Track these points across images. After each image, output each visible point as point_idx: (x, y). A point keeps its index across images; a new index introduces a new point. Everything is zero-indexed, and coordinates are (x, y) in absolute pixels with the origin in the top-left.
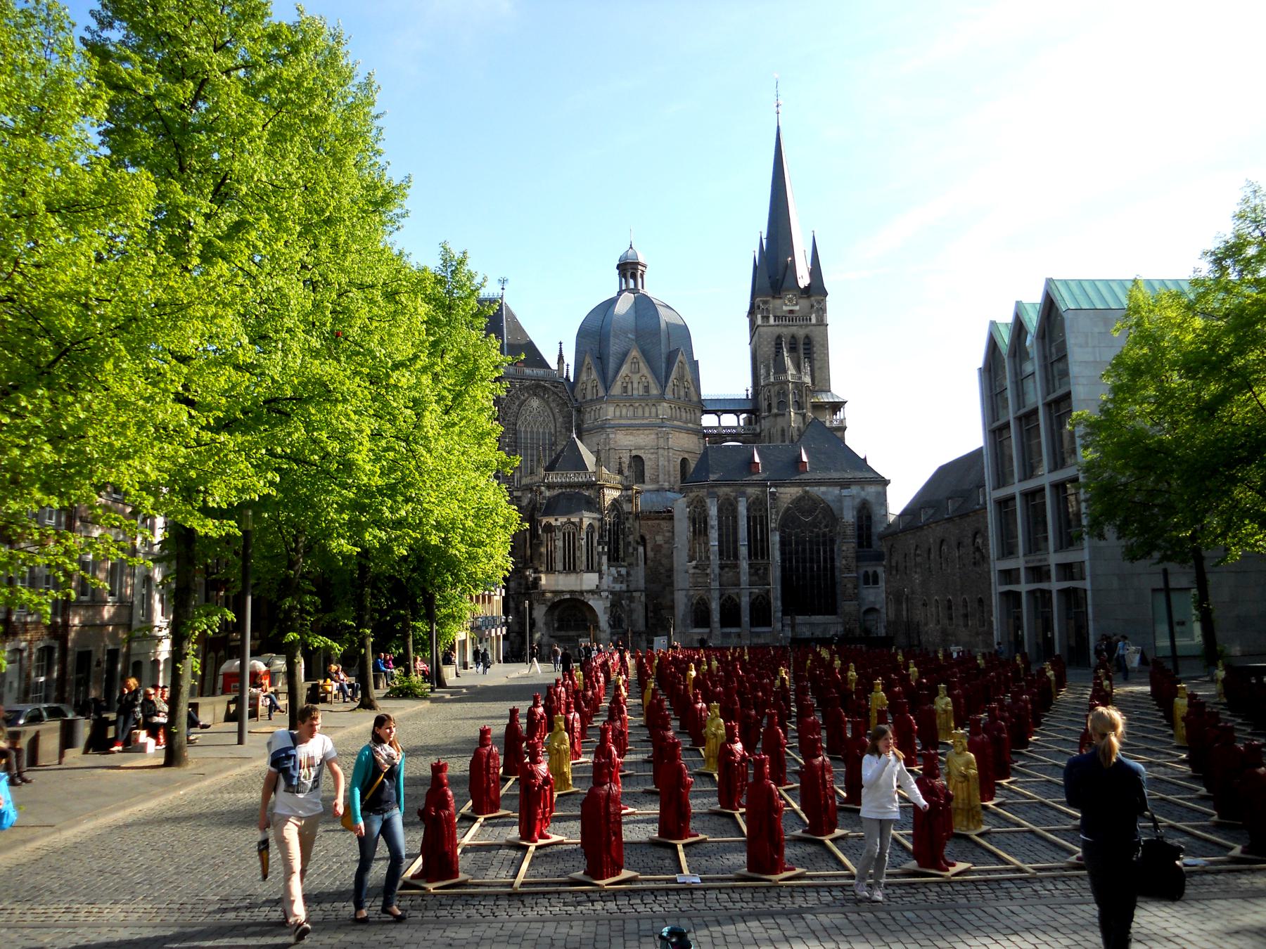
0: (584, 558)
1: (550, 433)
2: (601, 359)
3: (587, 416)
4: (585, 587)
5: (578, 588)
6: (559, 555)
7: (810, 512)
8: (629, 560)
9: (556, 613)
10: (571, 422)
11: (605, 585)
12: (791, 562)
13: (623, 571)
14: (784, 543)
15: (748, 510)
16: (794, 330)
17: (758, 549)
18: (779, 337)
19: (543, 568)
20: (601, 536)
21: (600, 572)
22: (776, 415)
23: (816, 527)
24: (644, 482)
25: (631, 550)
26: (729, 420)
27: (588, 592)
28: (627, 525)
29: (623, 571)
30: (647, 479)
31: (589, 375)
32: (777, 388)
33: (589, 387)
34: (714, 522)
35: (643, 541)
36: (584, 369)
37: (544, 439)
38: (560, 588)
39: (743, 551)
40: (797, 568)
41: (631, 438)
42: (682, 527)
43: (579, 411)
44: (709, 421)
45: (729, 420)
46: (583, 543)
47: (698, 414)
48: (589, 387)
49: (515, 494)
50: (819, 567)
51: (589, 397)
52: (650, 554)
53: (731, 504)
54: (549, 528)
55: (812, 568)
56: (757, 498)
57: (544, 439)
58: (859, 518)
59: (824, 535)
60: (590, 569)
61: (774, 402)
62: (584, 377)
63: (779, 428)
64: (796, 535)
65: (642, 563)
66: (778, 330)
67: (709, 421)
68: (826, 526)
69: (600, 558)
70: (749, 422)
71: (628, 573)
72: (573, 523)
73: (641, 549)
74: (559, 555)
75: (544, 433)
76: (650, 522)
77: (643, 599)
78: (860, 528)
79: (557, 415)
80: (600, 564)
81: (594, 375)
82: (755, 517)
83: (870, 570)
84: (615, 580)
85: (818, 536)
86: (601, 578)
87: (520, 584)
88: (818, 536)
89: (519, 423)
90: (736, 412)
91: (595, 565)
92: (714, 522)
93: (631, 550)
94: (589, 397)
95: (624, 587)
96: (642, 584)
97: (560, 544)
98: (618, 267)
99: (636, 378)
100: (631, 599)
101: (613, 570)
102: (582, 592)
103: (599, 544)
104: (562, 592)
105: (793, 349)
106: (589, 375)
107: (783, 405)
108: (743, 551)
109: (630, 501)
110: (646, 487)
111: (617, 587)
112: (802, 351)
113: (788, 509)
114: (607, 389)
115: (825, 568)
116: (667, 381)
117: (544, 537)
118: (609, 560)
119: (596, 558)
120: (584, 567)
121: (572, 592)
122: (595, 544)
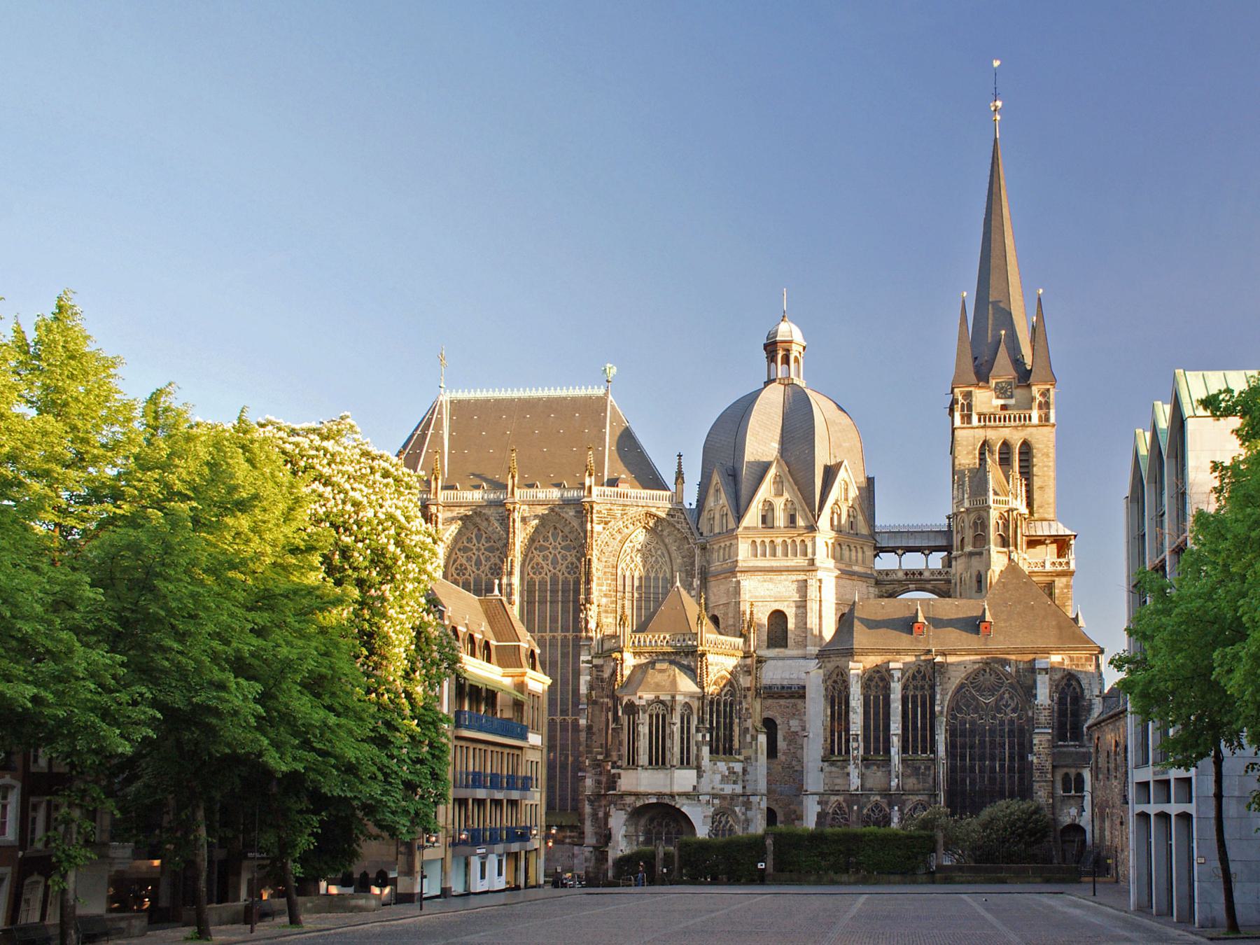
0: (677, 749)
1: (665, 579)
2: (733, 476)
3: (715, 555)
4: (676, 789)
5: (667, 790)
6: (643, 744)
7: (992, 690)
8: (745, 752)
9: (642, 822)
10: (693, 564)
11: (705, 787)
12: (963, 758)
13: (738, 767)
14: (952, 732)
15: (905, 688)
16: (1006, 433)
17: (918, 739)
18: (985, 443)
19: (625, 764)
20: (701, 720)
21: (698, 768)
22: (971, 554)
23: (999, 710)
24: (786, 646)
25: (748, 738)
26: (914, 561)
27: (680, 795)
28: (745, 705)
29: (738, 767)
30: (790, 642)
31: (717, 500)
32: (973, 516)
33: (717, 516)
34: (856, 701)
35: (770, 726)
36: (712, 491)
37: (657, 587)
38: (642, 789)
39: (896, 742)
40: (972, 769)
41: (771, 586)
42: (816, 709)
43: (704, 548)
44: (887, 562)
45: (914, 561)
46: (676, 729)
47: (869, 553)
48: (717, 516)
49: (596, 662)
50: (1002, 767)
51: (717, 531)
52: (781, 744)
53: (882, 679)
54: (631, 709)
55: (993, 769)
56: (919, 672)
57: (657, 587)
58: (1062, 701)
59: (1012, 721)
60: (685, 762)
61: (969, 534)
62: (710, 502)
63: (975, 574)
64: (973, 723)
65: (763, 758)
66: (981, 435)
67: (887, 562)
68: (1014, 711)
69: (699, 750)
70: (948, 563)
71: (744, 770)
72: (662, 702)
73: (762, 739)
74: (643, 744)
75: (656, 579)
76: (782, 702)
77: (764, 805)
78: (1062, 713)
79: (674, 554)
80: (698, 757)
81: (723, 500)
82: (915, 697)
83: (1072, 772)
84: (724, 779)
85: (1002, 723)
86: (699, 776)
87: (599, 782)
88: (1002, 723)
89: (622, 565)
90: (926, 550)
91: (693, 758)
92: (856, 701)
93: (748, 738)
94: (717, 531)
95: (738, 789)
96: (762, 786)
97: (644, 730)
98: (766, 346)
99: (779, 503)
100: (748, 805)
101: (722, 766)
102: (672, 796)
103: (698, 730)
104: (647, 795)
105: (1005, 461)
106: (717, 500)
107: (981, 538)
108: (896, 742)
109: (749, 673)
110: (787, 652)
111: (728, 789)
112: (1016, 465)
113: (962, 686)
114: (739, 518)
115: (1011, 769)
116: (821, 509)
117: (625, 720)
118: (711, 752)
119: (694, 749)
120: (676, 761)
121: (660, 795)
122: (693, 730)
